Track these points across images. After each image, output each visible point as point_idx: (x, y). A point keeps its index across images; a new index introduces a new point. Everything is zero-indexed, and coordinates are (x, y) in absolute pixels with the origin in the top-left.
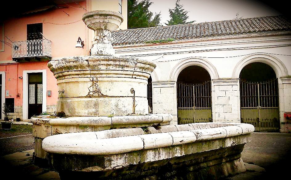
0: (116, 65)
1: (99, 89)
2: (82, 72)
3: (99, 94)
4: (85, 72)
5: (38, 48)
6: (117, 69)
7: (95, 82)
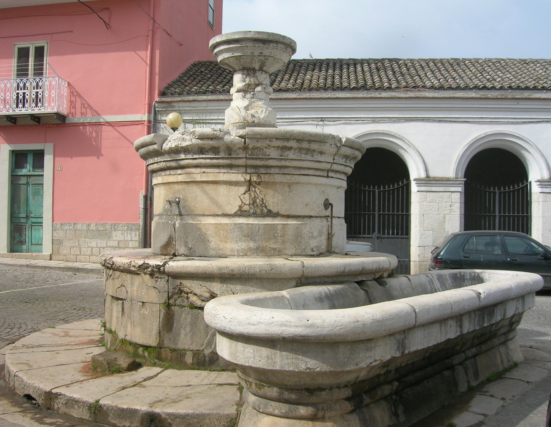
0: (301, 149)
5: (27, 96)
6: (303, 157)
7: (254, 184)
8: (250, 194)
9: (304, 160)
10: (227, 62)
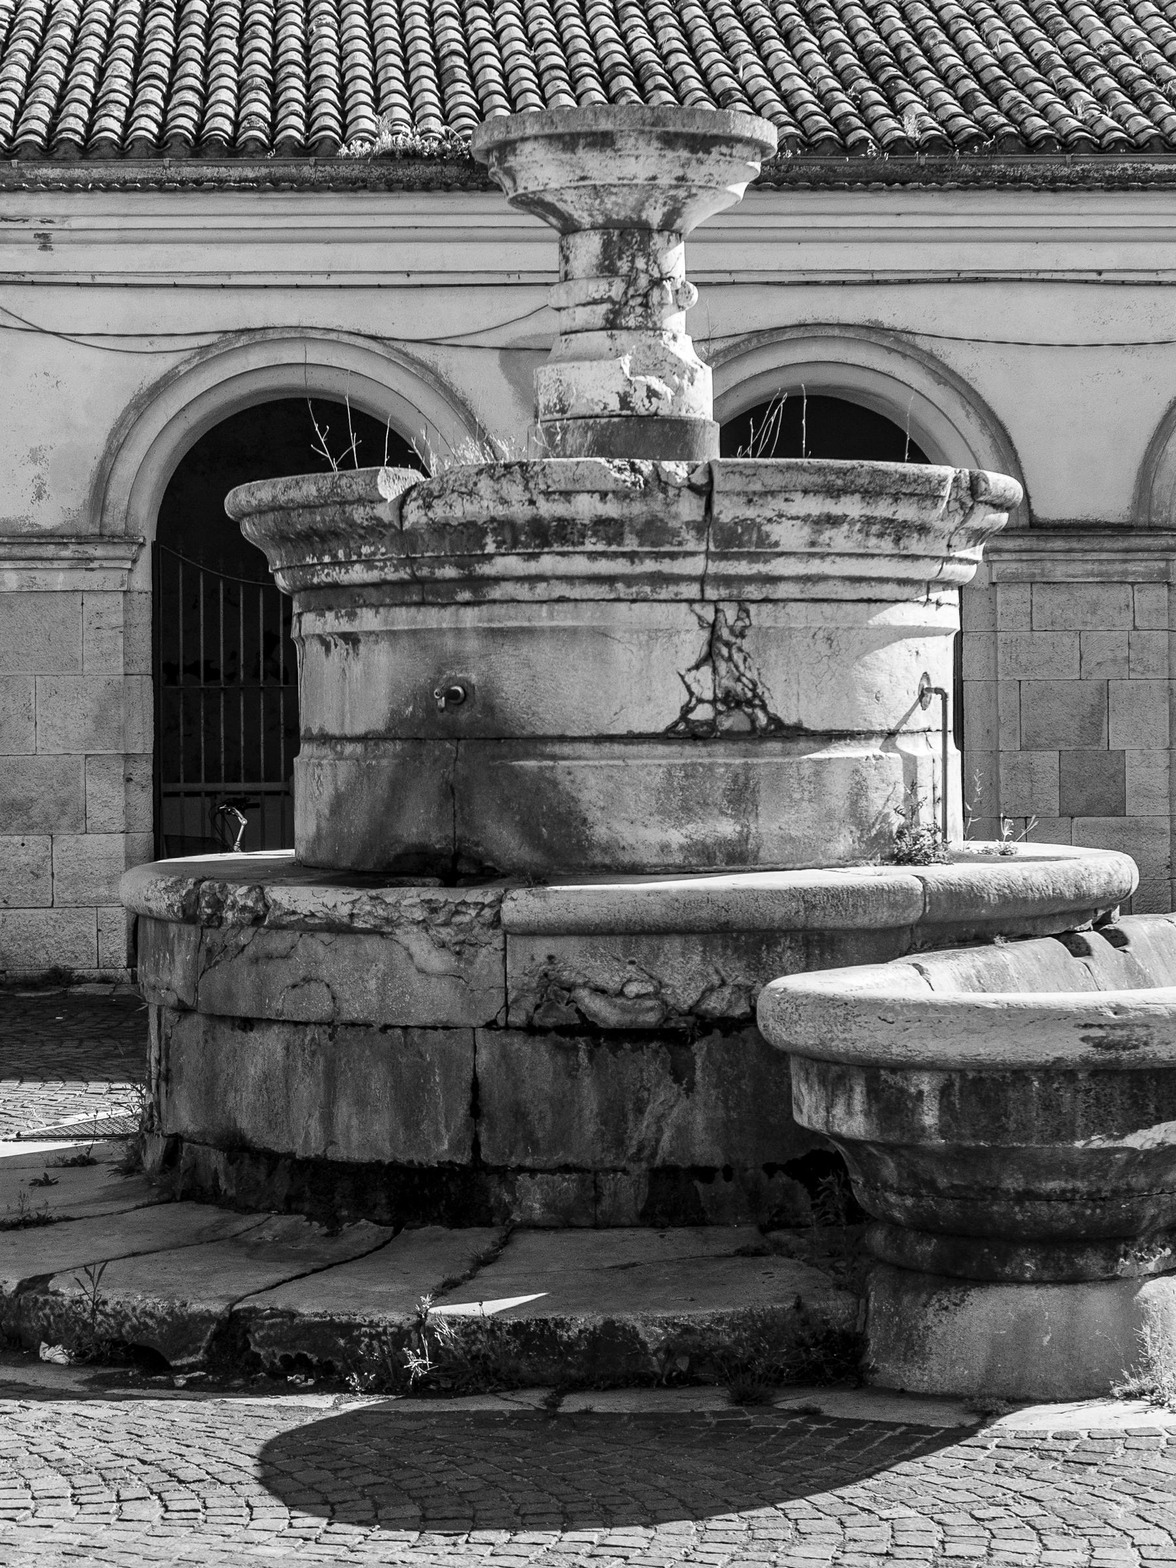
1: (755, 685)
2: (649, 566)
3: (753, 720)
4: (667, 566)
8: (715, 671)
9: (873, 556)
10: (549, 198)
